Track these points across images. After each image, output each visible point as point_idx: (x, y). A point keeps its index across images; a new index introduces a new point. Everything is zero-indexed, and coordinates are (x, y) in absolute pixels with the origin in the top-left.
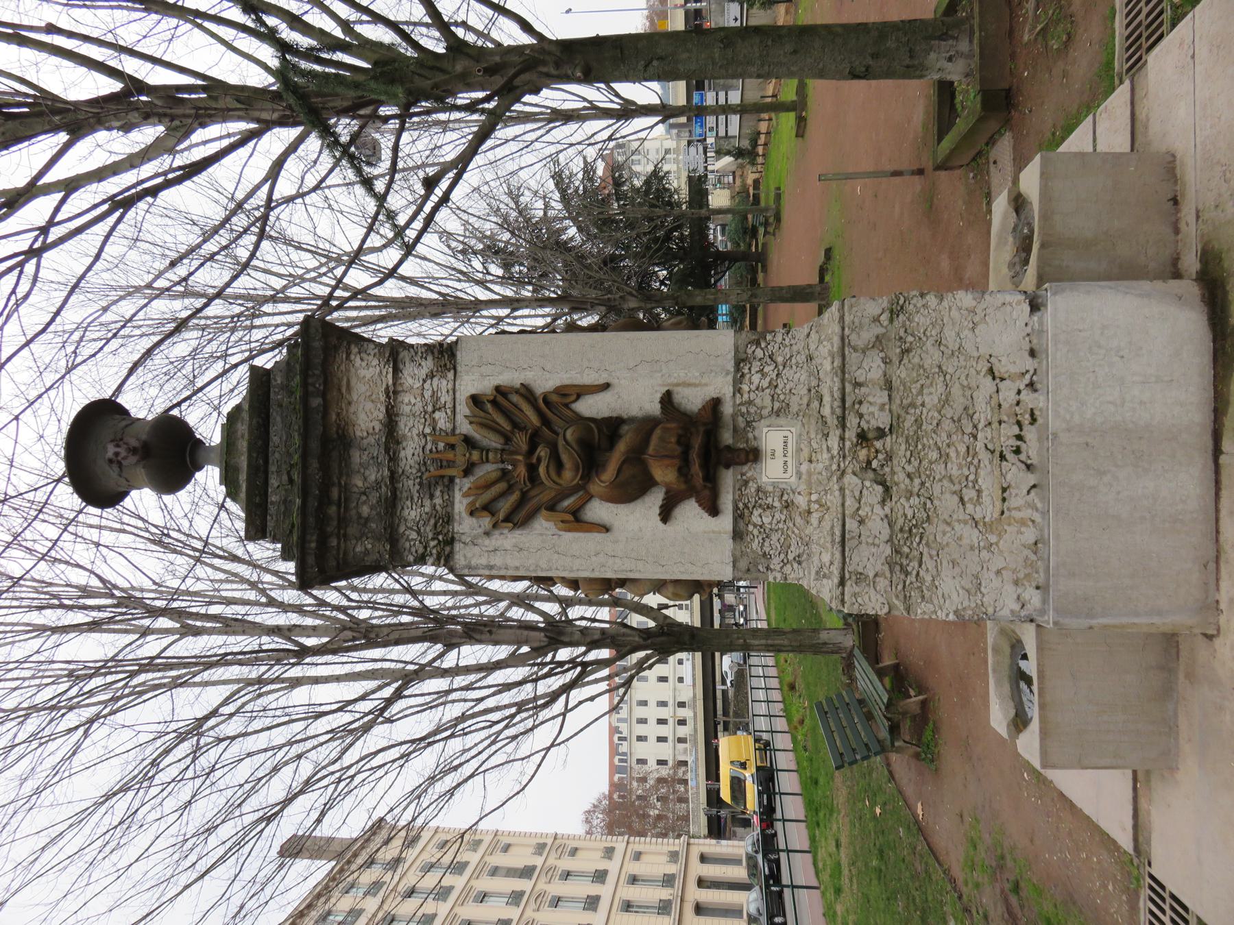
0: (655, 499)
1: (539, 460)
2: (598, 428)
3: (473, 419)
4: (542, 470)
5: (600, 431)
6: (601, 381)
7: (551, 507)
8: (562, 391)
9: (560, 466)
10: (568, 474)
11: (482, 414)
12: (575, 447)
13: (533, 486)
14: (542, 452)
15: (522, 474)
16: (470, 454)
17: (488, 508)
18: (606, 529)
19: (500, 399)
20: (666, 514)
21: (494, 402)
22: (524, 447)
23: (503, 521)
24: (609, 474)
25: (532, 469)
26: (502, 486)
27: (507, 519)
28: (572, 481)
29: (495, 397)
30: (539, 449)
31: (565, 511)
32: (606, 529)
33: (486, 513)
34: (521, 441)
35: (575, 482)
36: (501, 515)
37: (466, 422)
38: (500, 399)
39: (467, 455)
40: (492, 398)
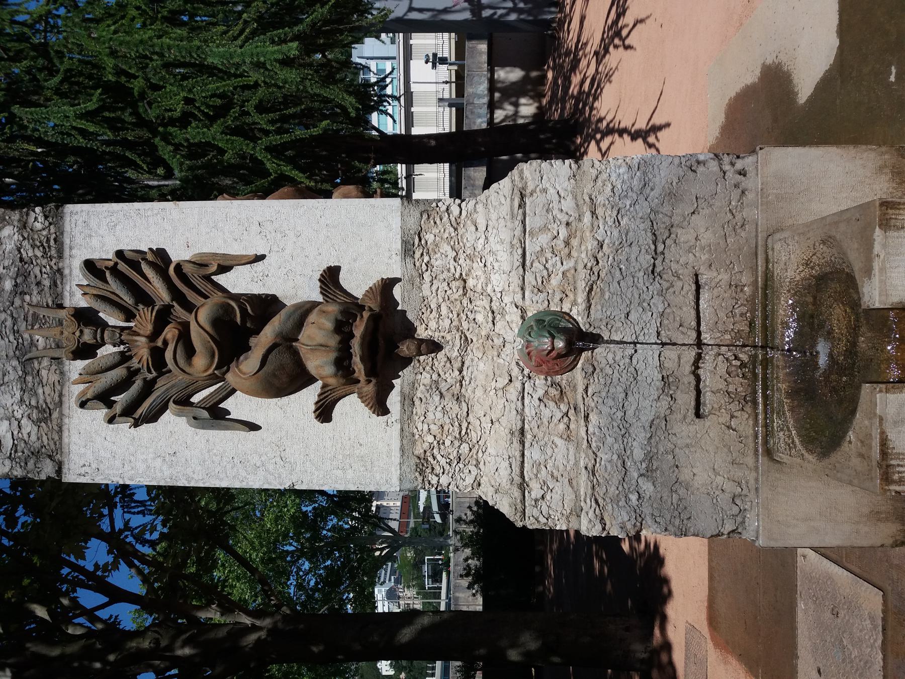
0: (309, 396)
1: (166, 343)
2: (239, 307)
3: (88, 290)
4: (169, 355)
5: (243, 311)
6: (252, 252)
7: (184, 402)
8: (200, 264)
9: (190, 352)
10: (200, 362)
11: (99, 284)
12: (208, 328)
13: (161, 374)
14: (170, 332)
15: (145, 358)
16: (81, 332)
17: (105, 398)
18: (253, 427)
19: (122, 267)
20: (324, 412)
21: (114, 270)
22: (149, 328)
23: (120, 416)
24: (250, 363)
25: (157, 355)
26: (119, 373)
27: (128, 412)
28: (206, 371)
29: (116, 264)
30: (166, 330)
31: (199, 406)
32: (253, 427)
33: (101, 405)
34: (145, 320)
35: (210, 371)
36: (118, 408)
37: (78, 293)
38: (122, 267)
39: (78, 334)
40: (111, 264)
